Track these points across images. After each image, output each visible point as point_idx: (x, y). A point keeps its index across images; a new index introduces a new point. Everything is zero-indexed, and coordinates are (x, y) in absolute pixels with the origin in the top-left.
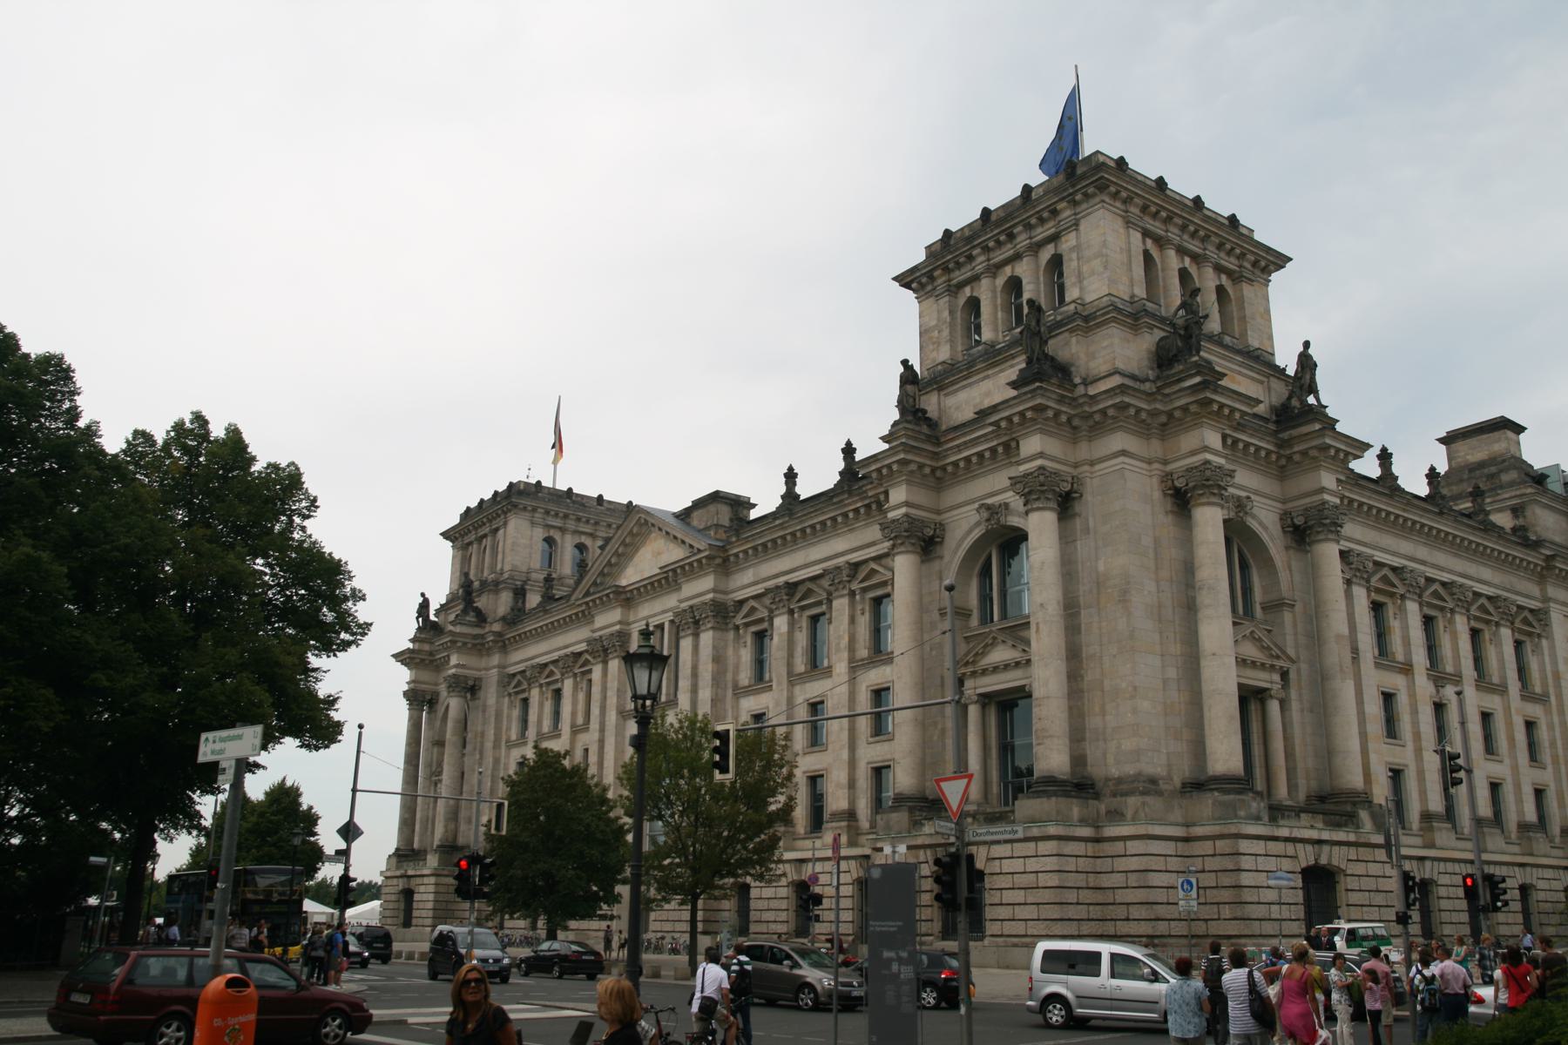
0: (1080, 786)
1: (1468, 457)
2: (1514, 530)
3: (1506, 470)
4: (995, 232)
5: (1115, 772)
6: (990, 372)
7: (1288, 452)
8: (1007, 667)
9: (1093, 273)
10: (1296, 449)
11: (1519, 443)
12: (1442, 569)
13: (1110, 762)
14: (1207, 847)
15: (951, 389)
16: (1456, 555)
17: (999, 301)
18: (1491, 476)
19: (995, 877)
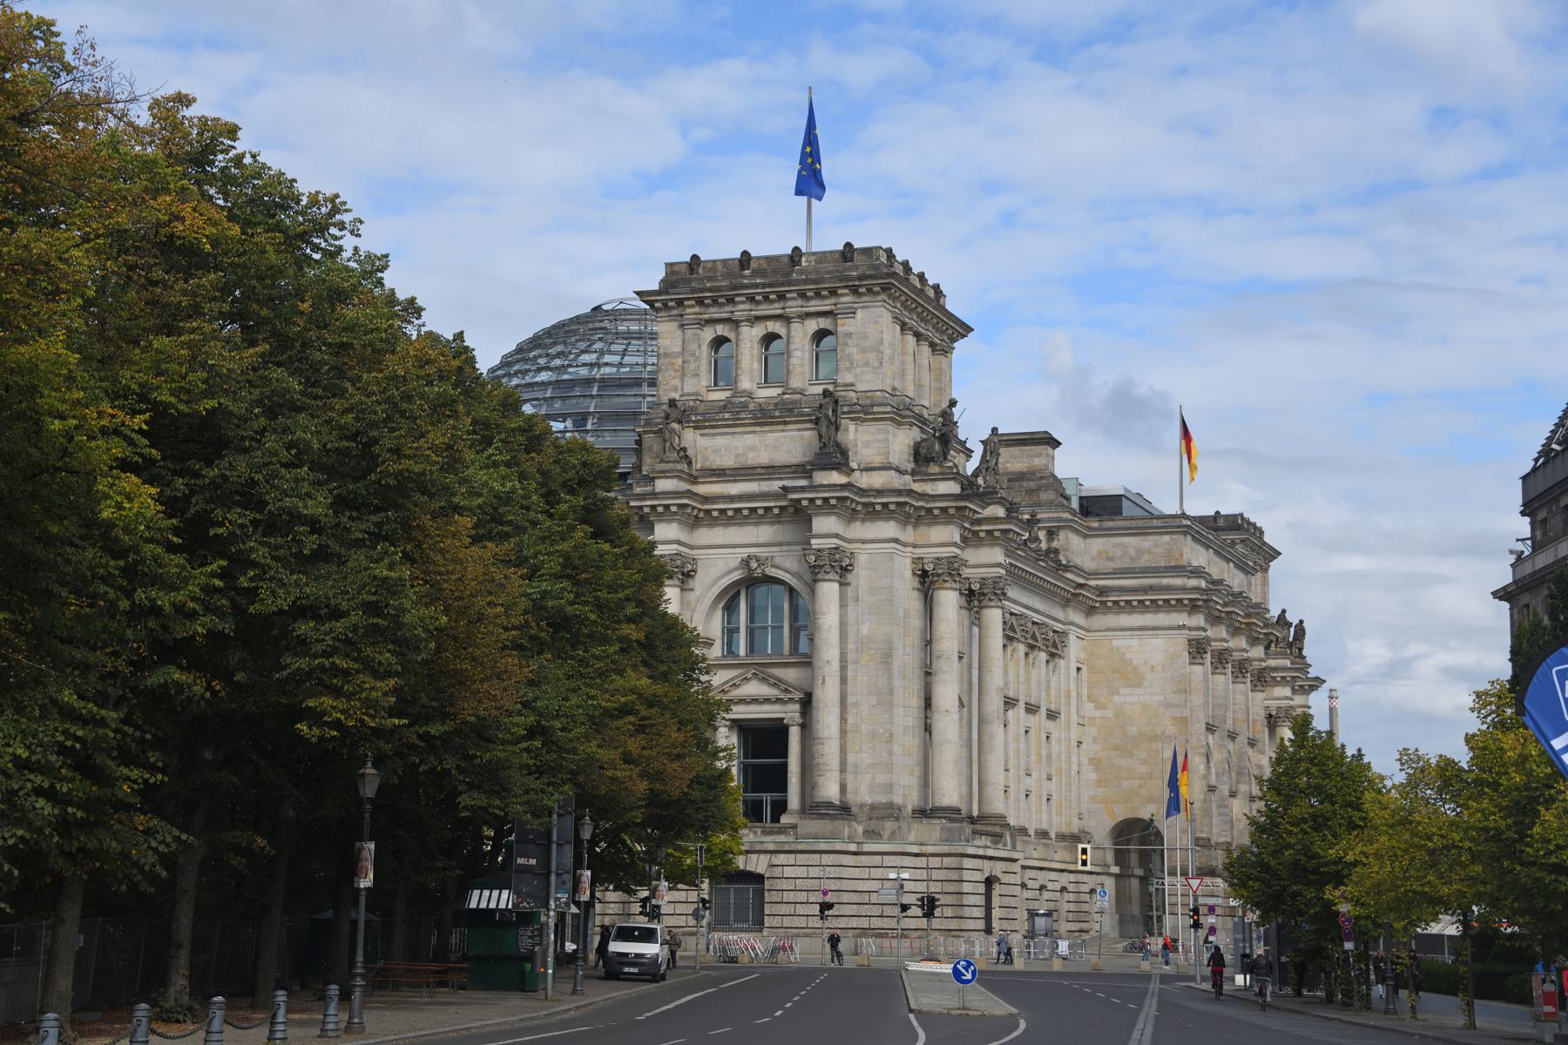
0: (844, 811)
1: (1009, 465)
2: (1048, 551)
3: (1047, 487)
4: (767, 290)
5: (868, 799)
6: (758, 429)
7: (976, 528)
8: (767, 701)
9: (867, 364)
10: (984, 528)
11: (1053, 458)
12: (1015, 602)
13: (863, 793)
14: (935, 862)
15: (707, 431)
16: (1024, 588)
17: (755, 351)
18: (1030, 492)
19: (776, 880)
